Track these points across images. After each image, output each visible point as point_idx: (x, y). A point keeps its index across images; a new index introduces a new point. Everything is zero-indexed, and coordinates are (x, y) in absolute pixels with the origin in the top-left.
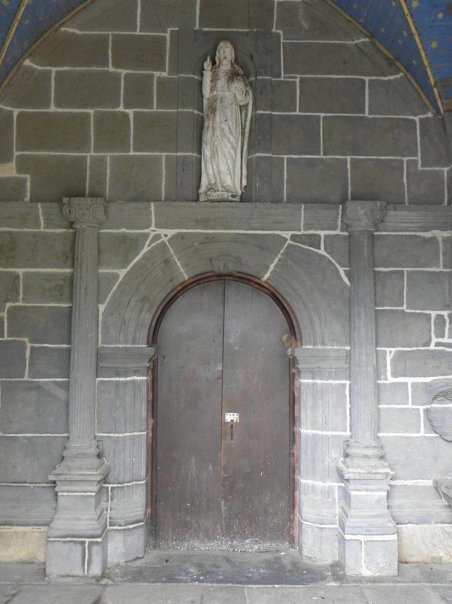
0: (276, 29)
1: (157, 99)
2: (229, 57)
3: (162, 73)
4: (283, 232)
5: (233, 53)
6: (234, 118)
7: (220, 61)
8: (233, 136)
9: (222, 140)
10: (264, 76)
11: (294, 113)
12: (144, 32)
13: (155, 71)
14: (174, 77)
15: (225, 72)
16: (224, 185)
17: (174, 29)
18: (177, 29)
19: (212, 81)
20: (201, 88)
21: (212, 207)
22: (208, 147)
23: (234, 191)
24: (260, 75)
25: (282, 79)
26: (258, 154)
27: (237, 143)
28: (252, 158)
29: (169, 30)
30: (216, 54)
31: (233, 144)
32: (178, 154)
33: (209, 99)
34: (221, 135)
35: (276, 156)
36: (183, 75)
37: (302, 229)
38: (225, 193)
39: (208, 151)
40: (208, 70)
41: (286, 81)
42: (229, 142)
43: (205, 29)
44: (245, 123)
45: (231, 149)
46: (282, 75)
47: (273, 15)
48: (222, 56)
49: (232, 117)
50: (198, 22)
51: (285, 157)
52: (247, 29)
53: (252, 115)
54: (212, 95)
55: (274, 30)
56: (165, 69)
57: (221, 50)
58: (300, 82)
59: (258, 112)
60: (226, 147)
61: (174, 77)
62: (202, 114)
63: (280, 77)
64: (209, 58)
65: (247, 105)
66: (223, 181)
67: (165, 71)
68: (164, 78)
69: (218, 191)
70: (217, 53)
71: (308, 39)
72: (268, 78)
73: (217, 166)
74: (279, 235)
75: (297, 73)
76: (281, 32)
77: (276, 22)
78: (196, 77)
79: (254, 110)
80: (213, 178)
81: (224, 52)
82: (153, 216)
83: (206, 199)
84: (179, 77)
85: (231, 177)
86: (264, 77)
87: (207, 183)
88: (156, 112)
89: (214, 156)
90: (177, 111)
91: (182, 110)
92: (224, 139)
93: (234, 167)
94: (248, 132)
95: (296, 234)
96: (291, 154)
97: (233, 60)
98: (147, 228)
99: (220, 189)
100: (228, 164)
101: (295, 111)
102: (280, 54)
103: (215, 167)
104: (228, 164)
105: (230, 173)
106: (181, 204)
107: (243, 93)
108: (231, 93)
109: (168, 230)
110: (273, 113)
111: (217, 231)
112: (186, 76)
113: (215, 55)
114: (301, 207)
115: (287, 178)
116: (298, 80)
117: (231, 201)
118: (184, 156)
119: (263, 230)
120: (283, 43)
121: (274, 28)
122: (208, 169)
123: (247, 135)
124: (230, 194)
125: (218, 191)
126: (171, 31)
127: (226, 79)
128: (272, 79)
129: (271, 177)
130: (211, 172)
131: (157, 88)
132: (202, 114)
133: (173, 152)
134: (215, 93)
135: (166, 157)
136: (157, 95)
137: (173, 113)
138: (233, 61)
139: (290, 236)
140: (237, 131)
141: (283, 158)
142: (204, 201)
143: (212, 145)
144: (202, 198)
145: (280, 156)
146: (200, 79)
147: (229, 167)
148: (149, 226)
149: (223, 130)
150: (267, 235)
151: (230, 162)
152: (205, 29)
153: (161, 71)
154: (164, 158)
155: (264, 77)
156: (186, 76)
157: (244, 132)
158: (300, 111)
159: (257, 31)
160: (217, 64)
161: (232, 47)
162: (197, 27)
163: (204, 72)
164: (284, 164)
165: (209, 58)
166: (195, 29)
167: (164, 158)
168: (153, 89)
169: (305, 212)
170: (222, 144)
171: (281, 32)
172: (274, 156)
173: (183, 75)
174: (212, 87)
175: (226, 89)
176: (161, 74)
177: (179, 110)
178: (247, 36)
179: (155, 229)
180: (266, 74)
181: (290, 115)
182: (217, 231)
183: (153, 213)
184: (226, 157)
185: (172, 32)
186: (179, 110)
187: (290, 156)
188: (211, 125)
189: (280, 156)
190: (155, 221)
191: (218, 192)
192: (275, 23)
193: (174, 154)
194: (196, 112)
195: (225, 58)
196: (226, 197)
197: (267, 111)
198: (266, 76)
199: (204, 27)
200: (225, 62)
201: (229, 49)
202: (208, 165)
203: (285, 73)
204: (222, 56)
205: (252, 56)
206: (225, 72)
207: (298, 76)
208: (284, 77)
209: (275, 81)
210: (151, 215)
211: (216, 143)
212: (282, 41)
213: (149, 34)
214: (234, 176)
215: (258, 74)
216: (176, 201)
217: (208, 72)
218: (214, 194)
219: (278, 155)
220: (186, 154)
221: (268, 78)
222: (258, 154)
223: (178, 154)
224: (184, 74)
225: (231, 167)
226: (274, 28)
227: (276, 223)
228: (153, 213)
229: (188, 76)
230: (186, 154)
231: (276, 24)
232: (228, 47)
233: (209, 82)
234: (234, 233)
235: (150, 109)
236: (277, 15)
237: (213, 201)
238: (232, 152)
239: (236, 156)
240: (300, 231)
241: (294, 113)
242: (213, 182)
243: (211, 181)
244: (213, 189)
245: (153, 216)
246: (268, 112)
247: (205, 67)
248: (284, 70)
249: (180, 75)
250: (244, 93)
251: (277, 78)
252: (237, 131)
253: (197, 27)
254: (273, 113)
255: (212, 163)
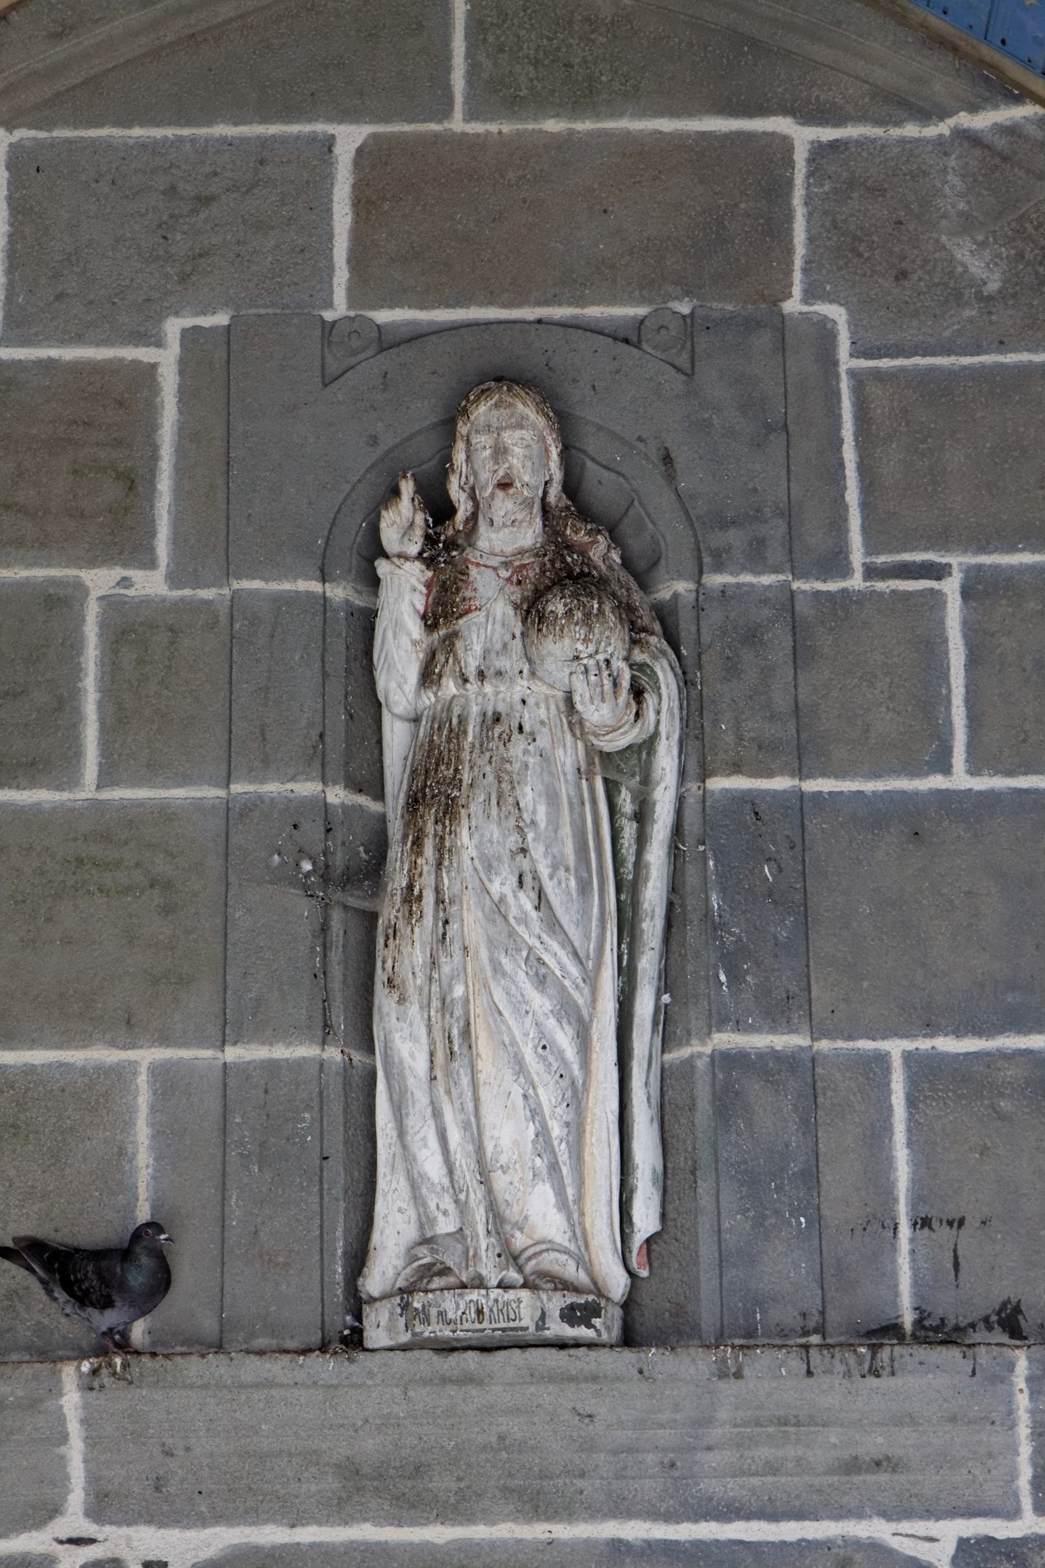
0: (811, 295)
1: (103, 730)
2: (527, 477)
3: (136, 575)
4: (905, 1527)
5: (554, 453)
6: (566, 831)
7: (473, 497)
8: (567, 942)
9: (497, 968)
10: (743, 569)
11: (936, 782)
12: (25, 342)
13: (92, 563)
14: (207, 594)
15: (506, 565)
16: (519, 1241)
17: (207, 321)
18: (221, 319)
19: (431, 621)
20: (368, 653)
21: (445, 1380)
22: (414, 1010)
23: (583, 1278)
24: (719, 567)
25: (856, 582)
26: (725, 1040)
27: (592, 980)
28: (690, 1062)
29: (173, 327)
30: (448, 458)
31: (564, 988)
32: (232, 1054)
33: (416, 720)
34: (491, 942)
35: (840, 1044)
36: (257, 584)
37: (1027, 1502)
38: (525, 1294)
39: (413, 1038)
40: (407, 558)
41: (880, 594)
42: (541, 981)
43: (383, 316)
44: (640, 853)
45: (551, 1023)
46: (857, 557)
47: (789, 218)
48: (487, 476)
49: (554, 824)
50: (341, 276)
51: (895, 1048)
52: (631, 301)
53: (680, 800)
54: (428, 698)
55: (793, 306)
56: (152, 550)
57: (481, 440)
58: (967, 593)
59: (718, 784)
60: (522, 1007)
61: (207, 594)
62: (375, 807)
63: (845, 571)
64: (407, 488)
65: (650, 744)
66: (513, 1214)
67: (151, 564)
68: (146, 602)
69: (479, 1283)
70: (459, 457)
71: (1002, 345)
72: (767, 580)
73: (466, 1126)
74: (876, 1548)
75: (942, 540)
76: (836, 313)
77: (808, 262)
78: (333, 1054)
79: (692, 767)
80: (448, 1203)
81: (500, 452)
82: (75, 1450)
83: (405, 1338)
84: (235, 593)
85: (560, 1192)
86: (747, 578)
87: (411, 1233)
88: (98, 807)
89: (448, 1074)
90: (222, 793)
91: (251, 788)
92: (506, 962)
93: (577, 1130)
94: (660, 912)
95: (991, 1540)
96: (931, 1029)
97: (555, 492)
98: (39, 1524)
99: (489, 1269)
100: (535, 1113)
101: (946, 769)
102: (841, 442)
103: (455, 1136)
104: (535, 1113)
105: (554, 1167)
106: (252, 1368)
107: (616, 684)
108: (544, 689)
109: (174, 1534)
110: (811, 786)
111: (479, 1532)
112: (274, 586)
113: (444, 468)
114: (1011, 1367)
115: (916, 1181)
116: (951, 587)
117: (562, 1345)
118: (272, 1067)
119: (774, 1517)
120: (852, 373)
121: (797, 290)
122: (415, 1147)
123: (652, 929)
124: (556, 1303)
125: (479, 1283)
126: (185, 333)
127: (516, 607)
128: (795, 586)
129: (811, 1177)
130: (432, 1165)
131: (102, 664)
132: (375, 807)
133: (202, 1042)
134: (450, 687)
135: (157, 1071)
136: (101, 706)
137: (198, 806)
138: (552, 499)
139: (949, 1548)
140: (586, 912)
141: (882, 1060)
142: (391, 1349)
143: (436, 1004)
144: (376, 1335)
145: (865, 1045)
146: (359, 602)
147: (543, 1133)
148: (53, 1511)
149: (499, 907)
150: (804, 1546)
151: (548, 1095)
152: (383, 316)
153: (125, 566)
154: (142, 1080)
155: (747, 578)
156: (274, 586)
157: (635, 904)
158: (974, 771)
159: (692, 313)
160: (460, 516)
161: (541, 422)
162: (339, 308)
163: (383, 567)
164: (889, 1092)
165: (407, 488)
166: (328, 316)
167: (142, 1080)
168: (77, 672)
169: (1034, 1395)
170: (499, 996)
171: (836, 313)
172: (824, 1045)
173: (257, 584)
174: (433, 654)
175: (511, 662)
176: (125, 582)
177: (236, 788)
178: (638, 346)
179: (88, 1529)
180: (756, 559)
181: (917, 793)
182: (479, 1532)
183: (74, 1428)
184: (520, 1068)
185: (190, 336)
186: (226, 591)
187: (924, 1044)
188: (427, 882)
189: (865, 1045)
190: (88, 1472)
191: (474, 1295)
192: (798, 263)
193: (208, 1053)
194: (337, 795)
195: (505, 485)
196: (527, 1319)
197: (770, 774)
198: (757, 573)
199: (373, 307)
200: (503, 506)
201: (527, 434)
202: (412, 1122)
203: (871, 547)
204: (484, 476)
205: (667, 459)
206: (506, 565)
207: (957, 561)
208: (871, 572)
209: (818, 594)
210: (64, 1438)
211: (459, 991)
212: (846, 361)
213: (54, 353)
214: (580, 1184)
215: (707, 559)
216: (219, 1347)
217: (408, 565)
218: (451, 1304)
219: (850, 1038)
220: (281, 1052)
221: (767, 580)
222: (725, 1040)
223: (232, 1054)
224: (266, 580)
225: (556, 1130)
226: (797, 290)
227: (852, 1466)
228: (74, 1428)
229: (287, 586)
230: (281, 1052)
231: (805, 271)
232: (520, 426)
233: (415, 628)
234: (587, 1542)
235: (58, 788)
236: (809, 217)
237: (446, 1348)
238: (564, 1039)
239: (585, 1063)
240: (1013, 1514)
241: (936, 782)
242: (446, 1226)
243: (432, 1222)
244: (446, 1271)
245: (75, 1450)
246: (781, 783)
247: (390, 536)
248: (865, 529)
249: (236, 585)
250: (626, 683)
251: (825, 575)
252: (586, 912)
253: (339, 308)
254: (811, 786)
255: (437, 1114)
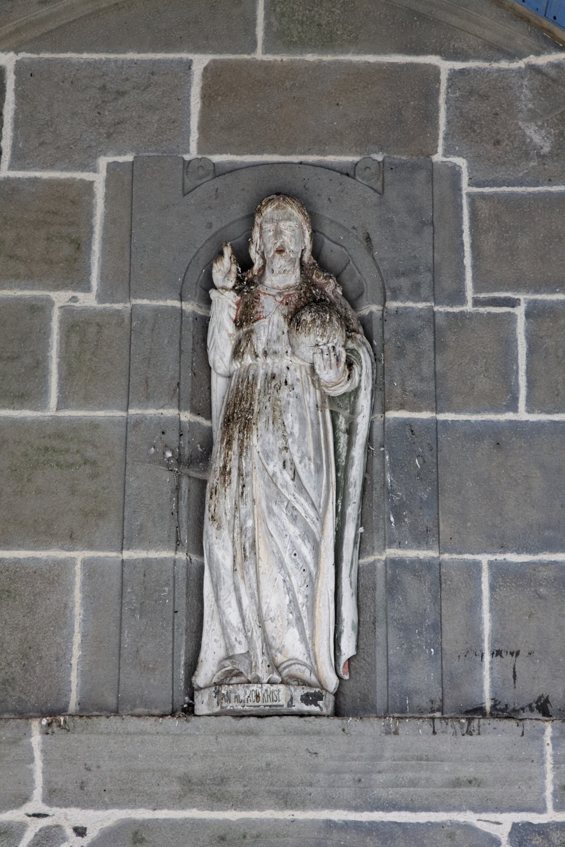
0: (447, 153)
1: (60, 378)
2: (292, 246)
3: (80, 295)
4: (484, 816)
5: (307, 234)
6: (309, 439)
7: (263, 257)
8: (308, 498)
9: (271, 511)
10: (408, 299)
11: (510, 416)
12: (23, 168)
13: (57, 288)
15: (280, 294)
16: (280, 658)
17: (121, 159)
18: (129, 158)
19: (239, 323)
20: (205, 340)
21: (238, 733)
22: (225, 533)
23: (313, 679)
24: (395, 298)
25: (469, 307)
26: (393, 552)
27: (322, 519)
28: (373, 564)
29: (103, 162)
30: (250, 236)
31: (306, 523)
32: (127, 555)
33: (230, 377)
35: (455, 556)
36: (145, 302)
37: (550, 805)
38: (282, 687)
39: (224, 548)
40: (227, 289)
41: (481, 314)
42: (294, 519)
43: (217, 158)
44: (349, 451)
45: (299, 541)
46: (470, 294)
47: (437, 110)
48: (271, 246)
49: (303, 435)
50: (194, 136)
51: (484, 559)
52: (350, 152)
53: (371, 423)
54: (236, 365)
55: (438, 158)
56: (89, 282)
57: (269, 227)
58: (528, 315)
59: (392, 415)
60: (284, 533)
63: (462, 301)
64: (227, 251)
65: (356, 392)
66: (276, 644)
67: (88, 289)
68: (85, 310)
69: (258, 681)
70: (256, 235)
71: (550, 182)
73: (252, 596)
74: (468, 828)
75: (518, 285)
76: (461, 162)
77: (447, 134)
78: (182, 556)
79: (378, 406)
81: (278, 233)
82: (38, 766)
83: (217, 709)
84: (133, 307)
85: (302, 632)
86: (410, 304)
87: (221, 653)
88: (57, 420)
89: (243, 568)
90: (124, 414)
91: (140, 412)
92: (275, 508)
93: (312, 599)
95: (530, 824)
96: (504, 548)
97: (307, 256)
99: (263, 673)
100: (290, 590)
101: (515, 409)
102: (462, 232)
103: (246, 601)
104: (290, 590)
105: (299, 619)
106: (133, 724)
107: (338, 360)
108: (299, 362)
109: (90, 813)
110: (442, 417)
111: (255, 815)
112: (155, 303)
114: (543, 731)
116: (520, 311)
117: (301, 715)
118: (146, 561)
119: (413, 809)
120: (469, 195)
121: (440, 149)
122: (224, 606)
124: (299, 692)
125: (258, 681)
126: (109, 165)
127: (285, 317)
128: (436, 309)
130: (233, 617)
133: (111, 548)
134: (248, 360)
135: (86, 563)
136: (59, 365)
137: (111, 421)
139: (507, 828)
140: (319, 482)
142: (209, 715)
143: (237, 530)
144: (201, 708)
145: (468, 557)
146: (201, 312)
147: (293, 601)
148: (25, 799)
149: (272, 479)
150: (430, 825)
151: (297, 580)
153: (74, 290)
154: (78, 568)
156: (155, 303)
157: (346, 478)
158: (530, 410)
160: (256, 267)
161: (300, 217)
163: (213, 294)
164: (480, 583)
165: (227, 251)
166: (187, 157)
167: (78, 568)
168: (46, 347)
169: (555, 747)
170: (271, 526)
171: (461, 162)
176: (74, 299)
177: (132, 411)
178: (354, 178)
179: (45, 809)
181: (499, 422)
182: (255, 815)
183: (37, 755)
184: (282, 565)
185: (112, 167)
186: (128, 305)
187: (500, 557)
188: (233, 464)
189: (468, 557)
191: (255, 687)
192: (441, 135)
193: (114, 554)
194: (186, 417)
195: (280, 251)
196: (283, 701)
197: (420, 410)
198: (415, 301)
199: (211, 153)
200: (279, 263)
201: (293, 224)
203: (477, 289)
204: (269, 246)
205: (368, 239)
206: (280, 294)
207: (524, 297)
208: (477, 302)
209: (448, 313)
210: (32, 760)
211: (250, 523)
212: (466, 188)
213: (38, 174)
215: (388, 293)
216: (116, 712)
217: (227, 293)
218: (241, 691)
219: (460, 553)
220: (153, 554)
221: (421, 305)
222: (393, 552)
223: (127, 555)
225: (301, 599)
226: (440, 149)
227: (457, 783)
228: (37, 755)
229: (161, 303)
230: (153, 554)
231: (445, 139)
232: (289, 219)
233: (230, 327)
234: (313, 821)
237: (239, 715)
238: (306, 550)
239: (317, 564)
240: (542, 810)
241: (510, 416)
242: (240, 650)
243: (232, 647)
244: (239, 674)
245: (38, 766)
246: (426, 415)
247: (218, 277)
248: (474, 279)
249: (134, 302)
250: (343, 359)
252: (319, 482)
254: (442, 417)
255: (237, 589)
